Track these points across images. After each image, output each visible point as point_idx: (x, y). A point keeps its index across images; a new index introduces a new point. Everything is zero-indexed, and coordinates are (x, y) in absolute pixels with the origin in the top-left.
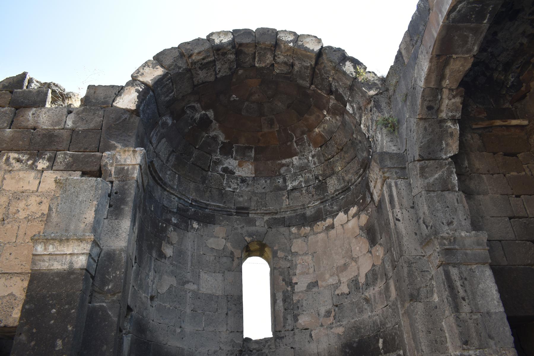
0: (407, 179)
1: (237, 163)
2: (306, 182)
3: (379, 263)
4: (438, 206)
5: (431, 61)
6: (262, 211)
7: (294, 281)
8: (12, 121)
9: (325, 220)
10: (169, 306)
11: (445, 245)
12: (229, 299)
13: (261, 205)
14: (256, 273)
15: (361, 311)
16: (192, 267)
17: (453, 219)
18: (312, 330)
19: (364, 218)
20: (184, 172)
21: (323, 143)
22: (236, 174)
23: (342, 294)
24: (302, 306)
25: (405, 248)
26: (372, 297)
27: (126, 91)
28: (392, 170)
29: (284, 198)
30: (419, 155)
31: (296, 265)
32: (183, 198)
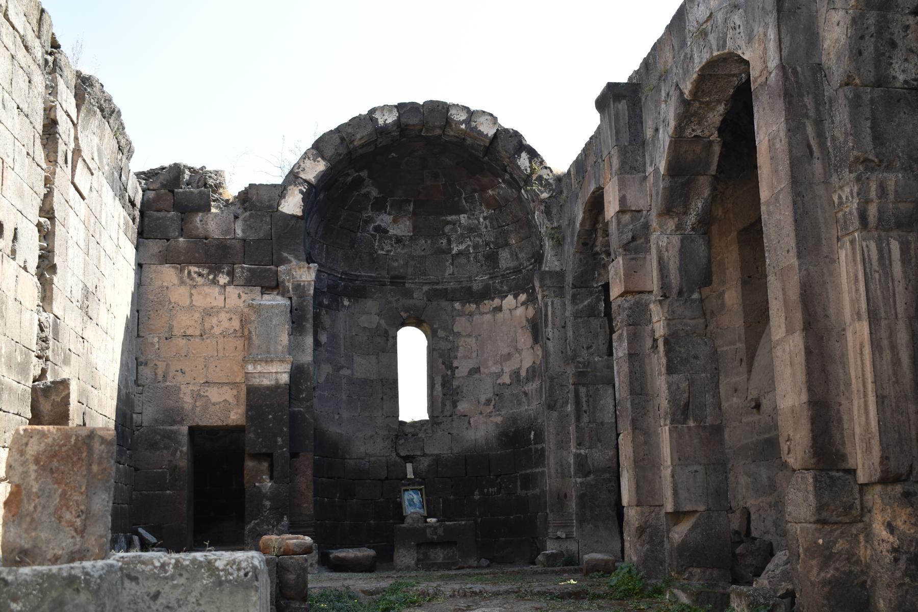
2: (476, 247)
3: (538, 362)
5: (584, 213)
8: (182, 230)
15: (520, 403)
19: (531, 312)
21: (498, 205)
23: (504, 384)
27: (290, 192)
29: (447, 264)
31: (458, 347)
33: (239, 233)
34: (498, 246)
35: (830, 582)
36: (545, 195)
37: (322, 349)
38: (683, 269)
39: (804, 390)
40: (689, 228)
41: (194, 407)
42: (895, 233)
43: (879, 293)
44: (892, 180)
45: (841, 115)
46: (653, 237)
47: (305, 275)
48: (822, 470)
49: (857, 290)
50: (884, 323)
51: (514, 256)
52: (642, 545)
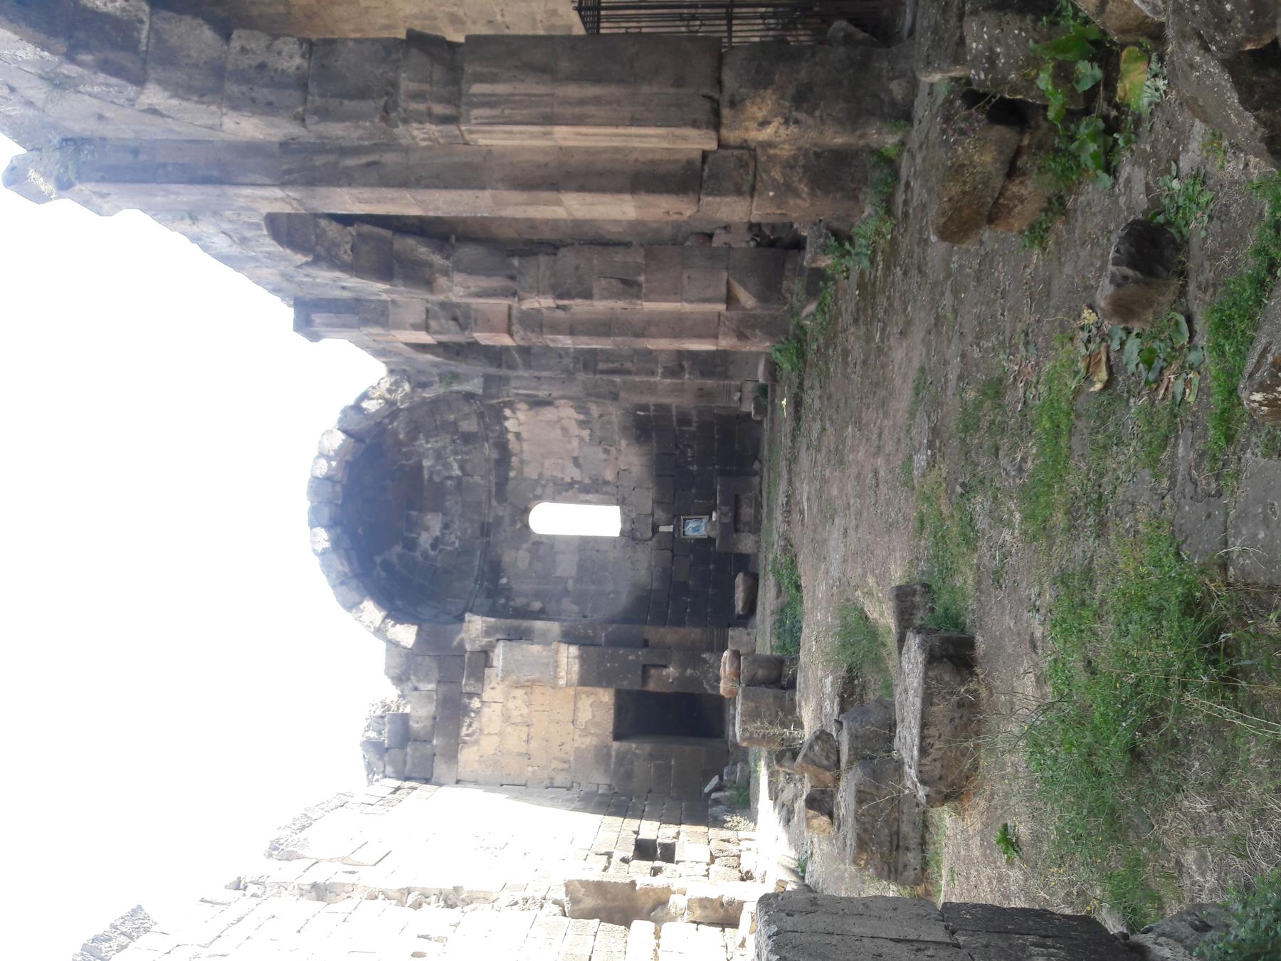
2: (456, 453)
3: (571, 403)
9: (508, 441)
14: (553, 519)
15: (610, 422)
19: (523, 406)
33: (432, 686)
34: (456, 431)
35: (812, 189)
36: (407, 387)
38: (488, 272)
39: (620, 196)
40: (447, 262)
41: (596, 735)
42: (464, 87)
43: (525, 111)
44: (407, 83)
45: (337, 130)
46: (455, 299)
47: (475, 627)
48: (701, 187)
49: (521, 133)
50: (557, 110)
51: (466, 417)
52: (755, 336)
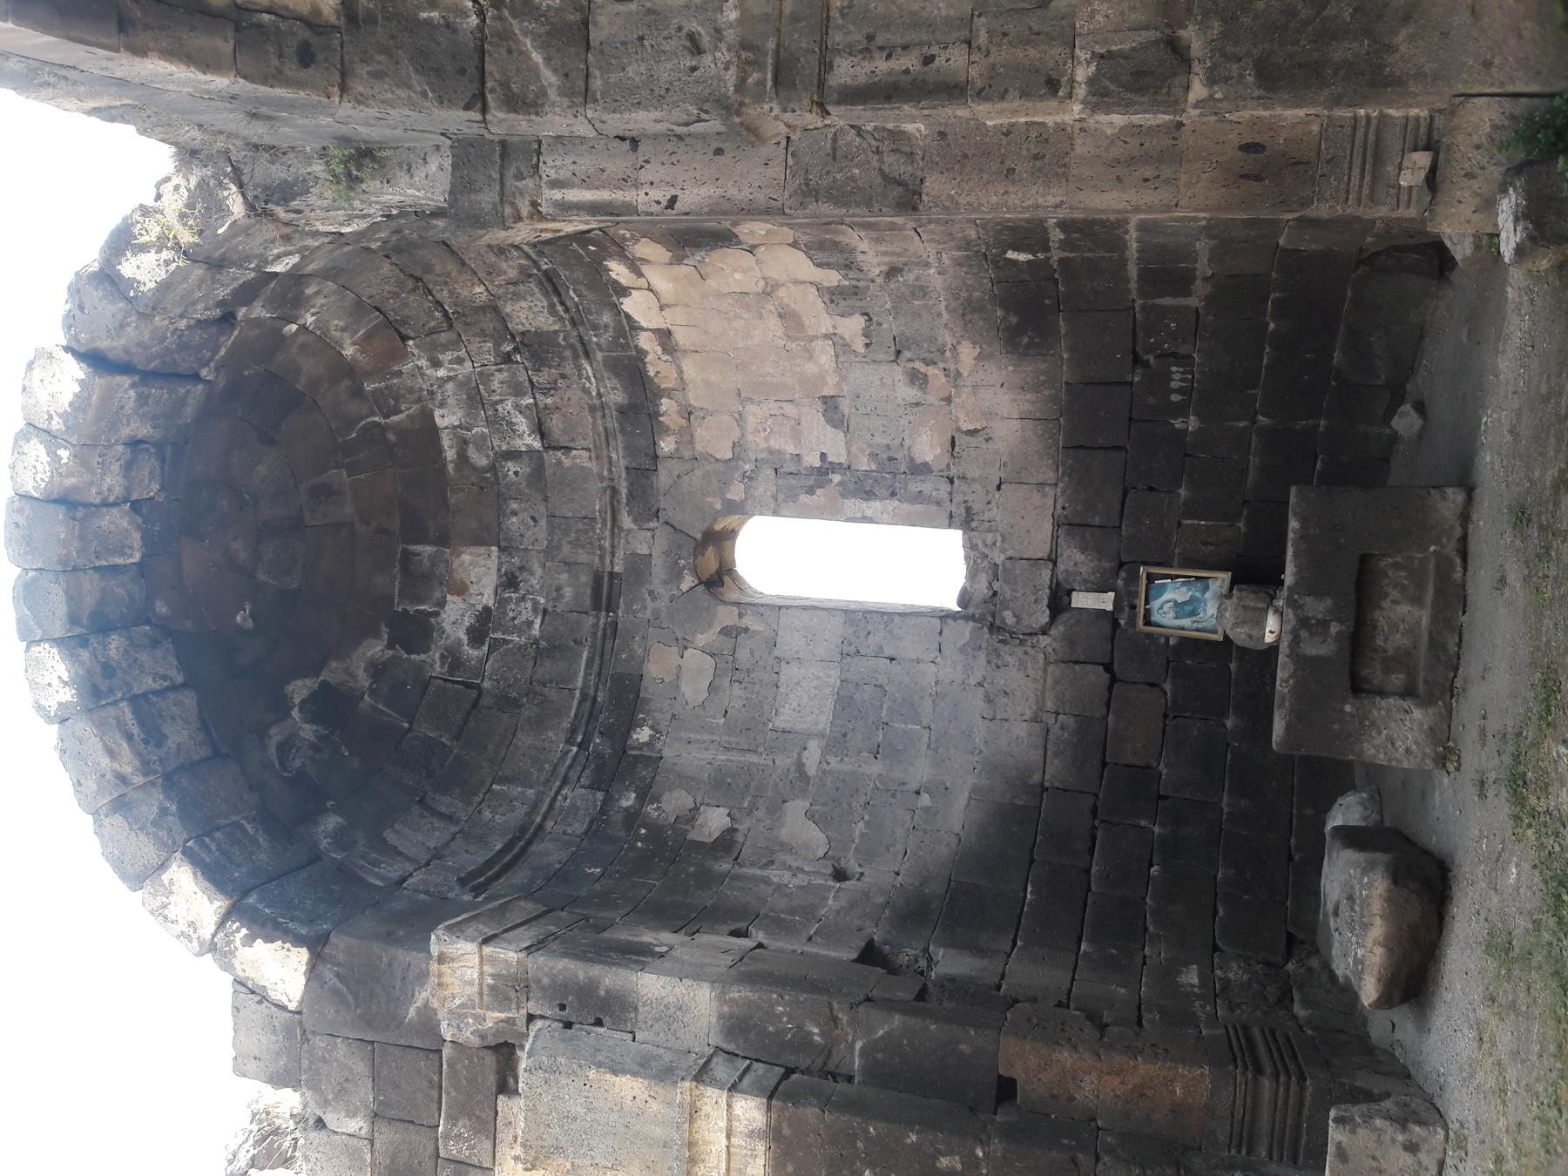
0: (540, 143)
1: (455, 598)
2: (518, 392)
3: (789, 235)
4: (635, 71)
6: (607, 533)
7: (817, 463)
9: (642, 353)
10: (861, 825)
11: (762, 83)
12: (852, 649)
13: (586, 532)
15: (921, 291)
16: (761, 749)
17: (680, 29)
18: (958, 429)
20: (484, 764)
21: (392, 333)
22: (491, 603)
23: (866, 335)
24: (888, 447)
25: (760, 197)
26: (886, 259)
28: (508, 190)
29: (567, 462)
30: (467, 108)
31: (771, 451)
32: (563, 770)
33: (357, 1124)
34: (503, 330)
37: (742, 827)
